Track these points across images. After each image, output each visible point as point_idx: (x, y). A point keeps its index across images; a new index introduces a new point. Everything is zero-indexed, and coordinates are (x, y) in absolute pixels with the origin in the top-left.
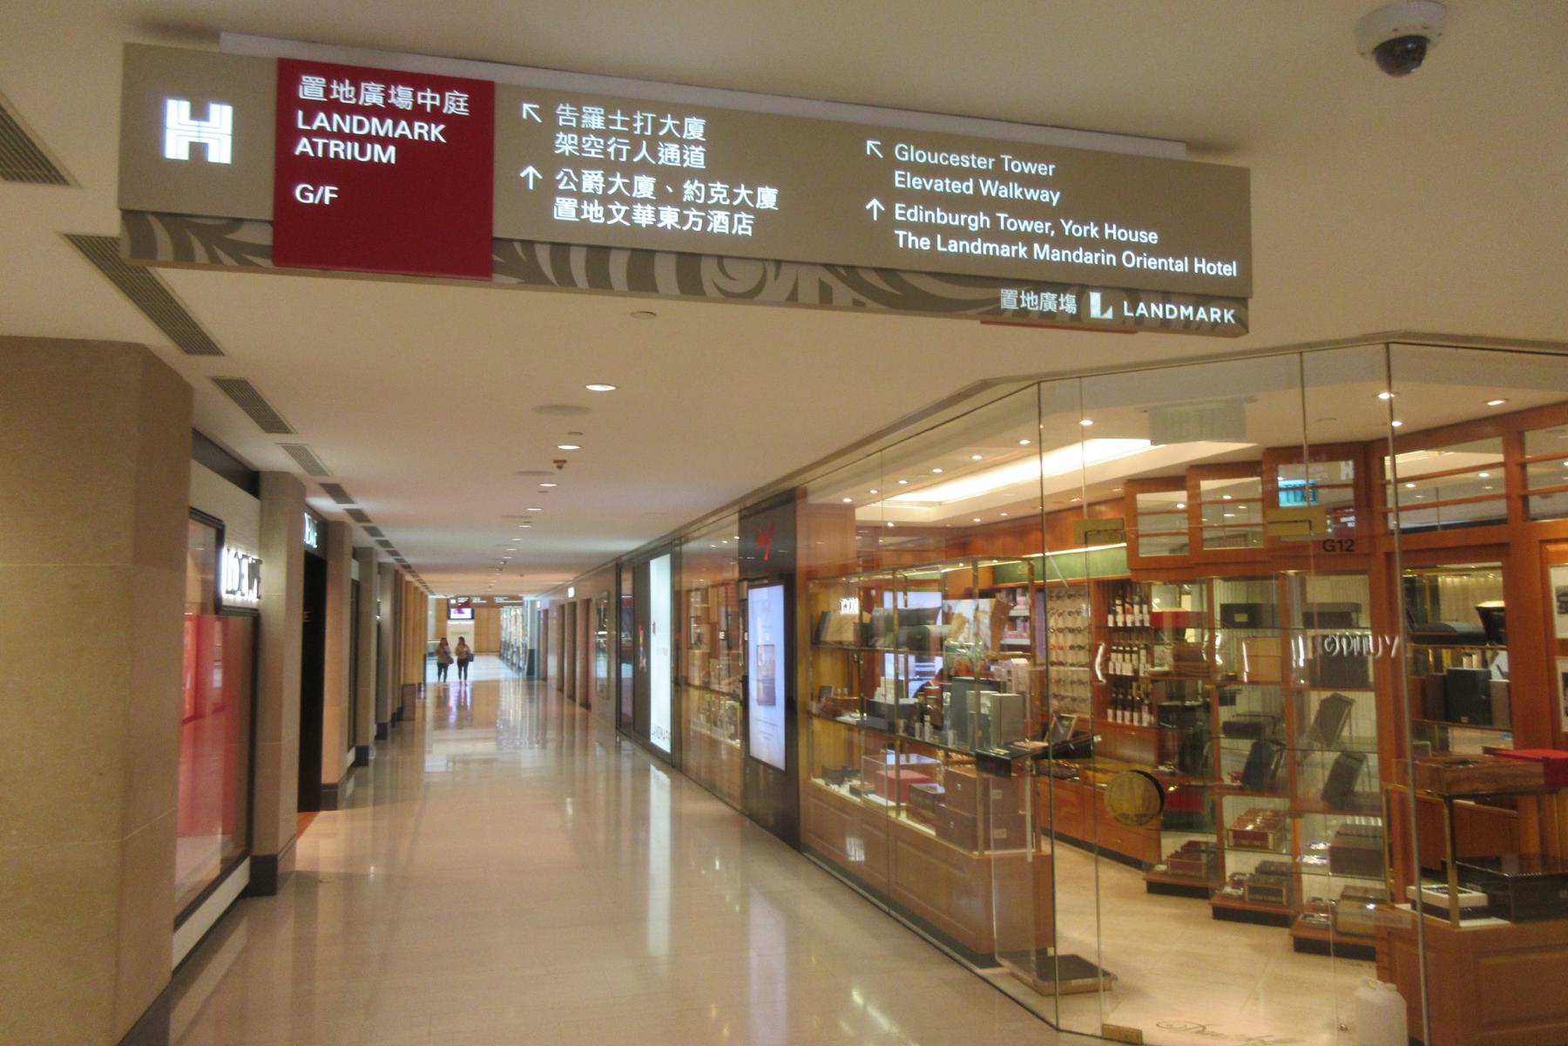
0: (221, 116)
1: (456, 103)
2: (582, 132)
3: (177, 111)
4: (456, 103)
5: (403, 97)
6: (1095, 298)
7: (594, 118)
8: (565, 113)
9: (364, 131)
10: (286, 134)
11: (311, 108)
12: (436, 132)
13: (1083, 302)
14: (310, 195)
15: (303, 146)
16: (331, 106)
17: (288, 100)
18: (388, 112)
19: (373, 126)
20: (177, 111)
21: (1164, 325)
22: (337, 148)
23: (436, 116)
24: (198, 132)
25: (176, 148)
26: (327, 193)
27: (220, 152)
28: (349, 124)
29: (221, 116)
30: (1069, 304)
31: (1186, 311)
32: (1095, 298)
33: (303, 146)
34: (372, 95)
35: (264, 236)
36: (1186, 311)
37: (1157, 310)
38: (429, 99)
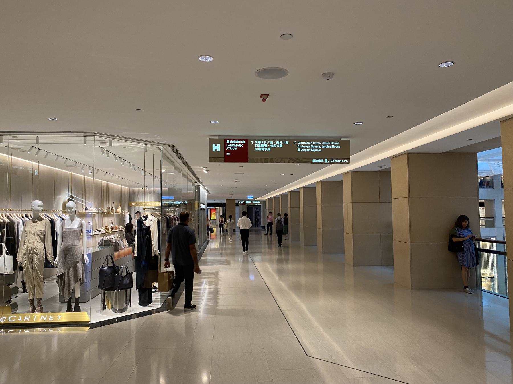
0: (219, 145)
1: (244, 142)
2: (258, 144)
3: (214, 145)
4: (244, 142)
5: (238, 142)
6: (326, 160)
7: (260, 142)
8: (256, 142)
9: (234, 146)
10: (226, 147)
11: (228, 144)
12: (241, 146)
13: (325, 161)
14: (227, 154)
15: (227, 149)
16: (230, 144)
17: (225, 143)
18: (236, 144)
19: (235, 145)
20: (214, 145)
21: (337, 163)
22: (231, 148)
23: (242, 144)
24: (217, 148)
25: (214, 150)
26: (229, 154)
27: (219, 150)
28: (232, 145)
29: (219, 145)
30: (323, 161)
31: (340, 161)
32: (326, 160)
33: (227, 149)
34: (234, 142)
35: (223, 159)
36: (340, 161)
37: (336, 161)
38: (241, 142)
